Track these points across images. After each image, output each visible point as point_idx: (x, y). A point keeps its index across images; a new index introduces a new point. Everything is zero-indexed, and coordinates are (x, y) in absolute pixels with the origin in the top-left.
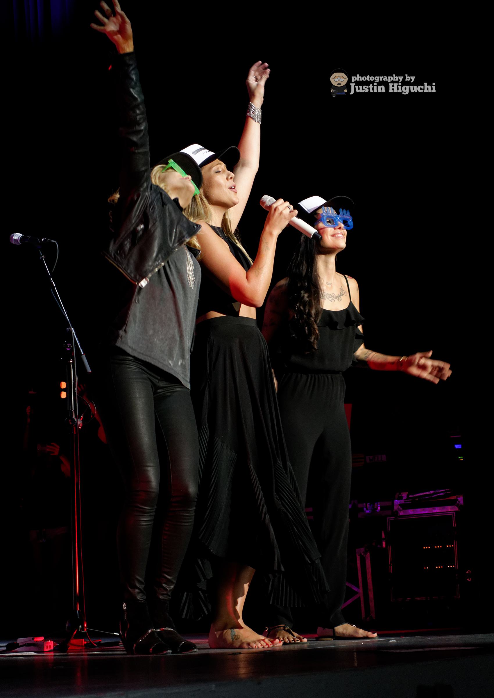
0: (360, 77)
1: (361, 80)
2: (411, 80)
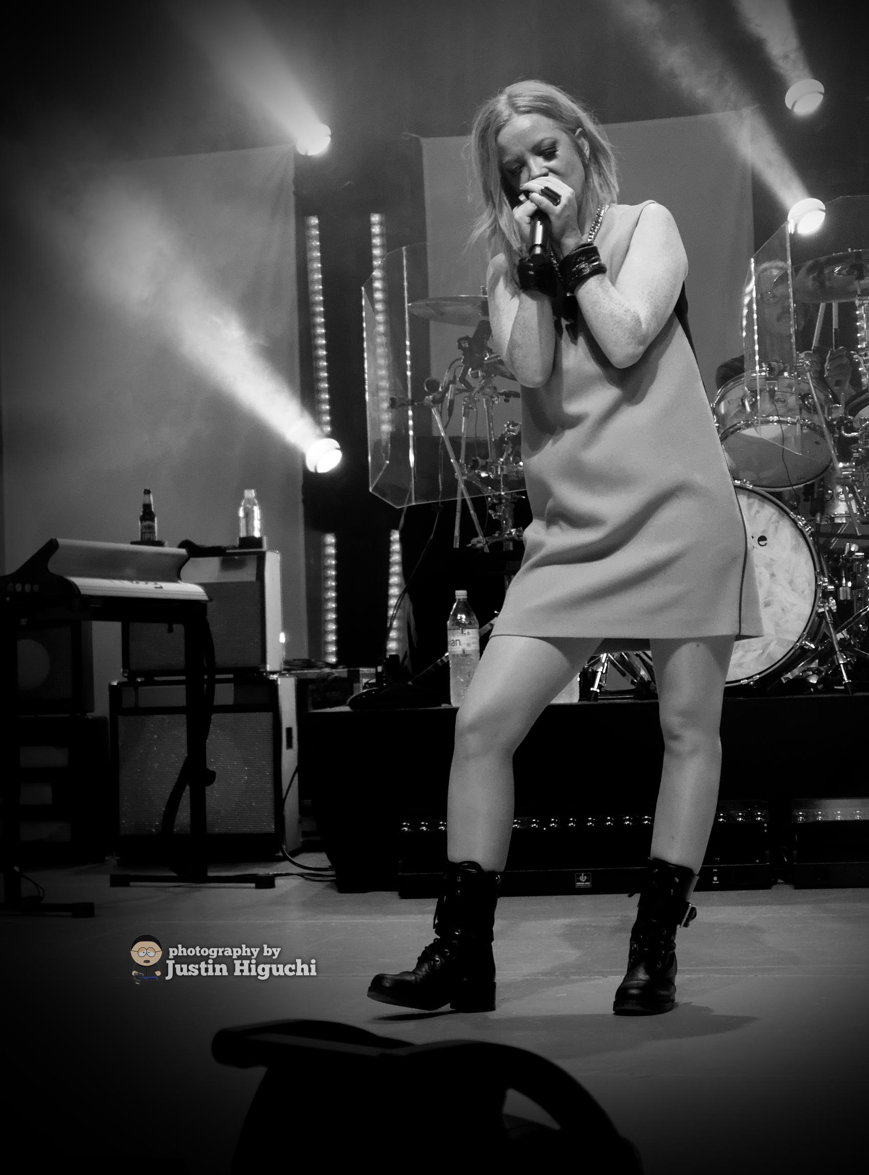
0: (184, 950)
1: (185, 954)
2: (273, 954)
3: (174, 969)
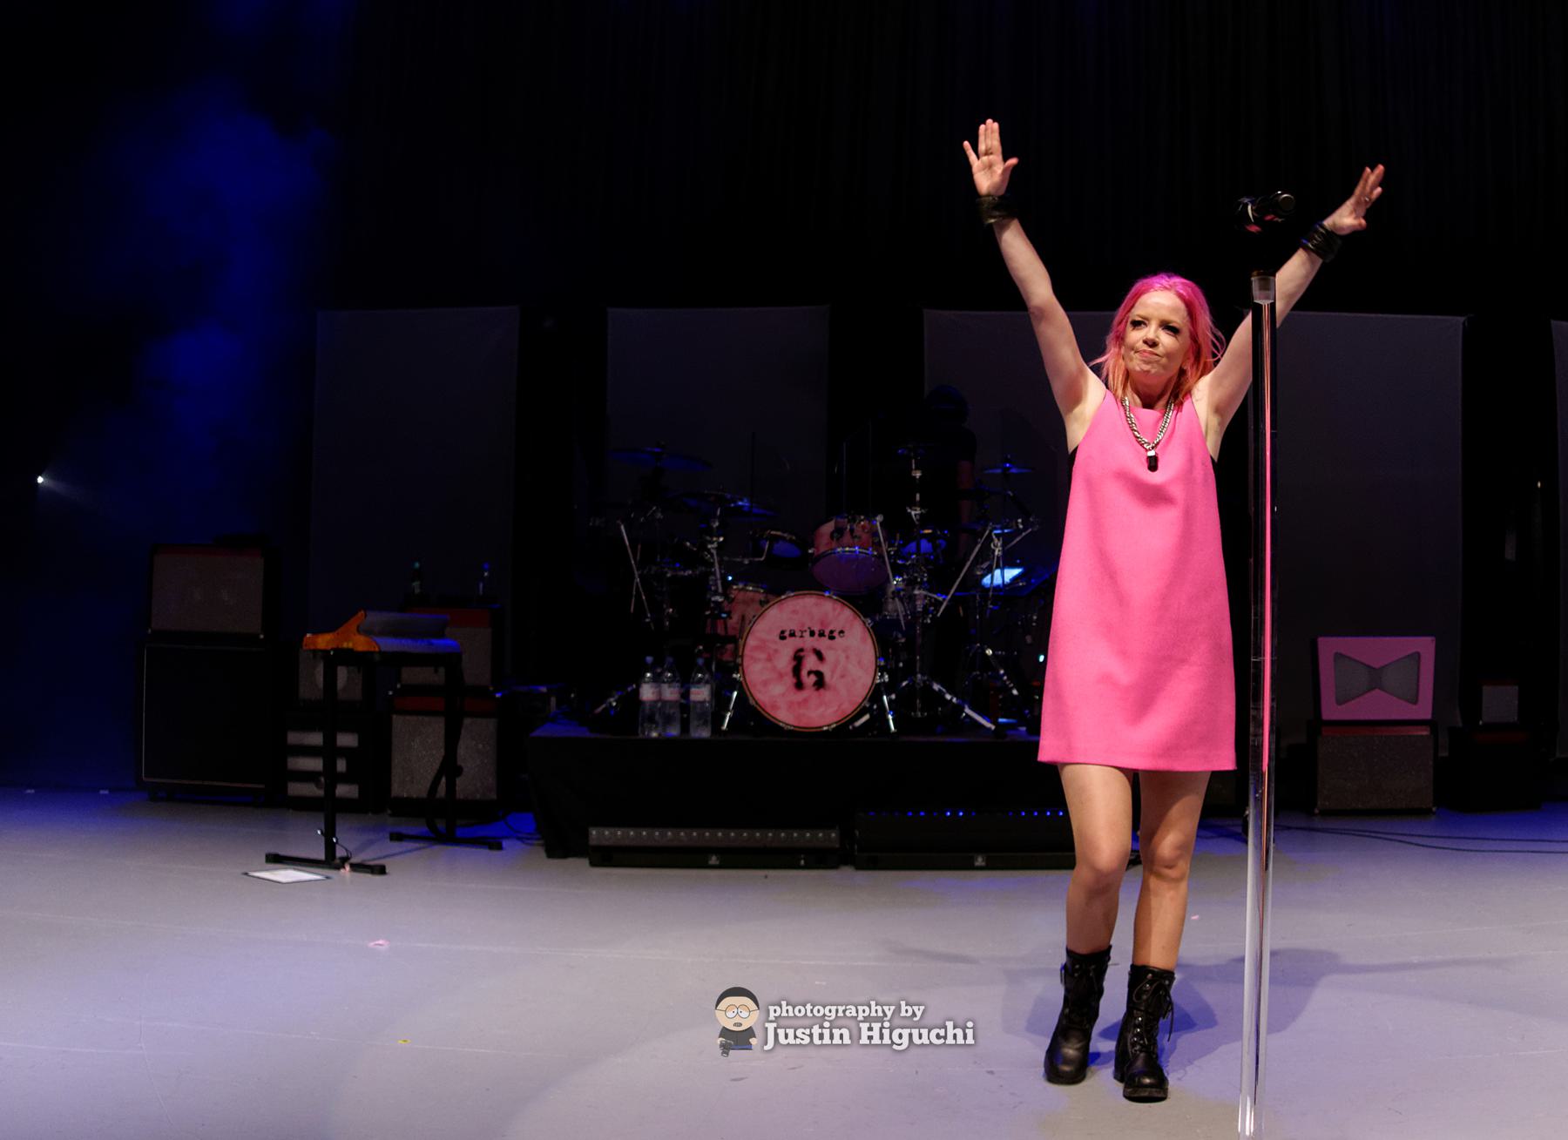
2: (914, 1014)
3: (776, 1035)
